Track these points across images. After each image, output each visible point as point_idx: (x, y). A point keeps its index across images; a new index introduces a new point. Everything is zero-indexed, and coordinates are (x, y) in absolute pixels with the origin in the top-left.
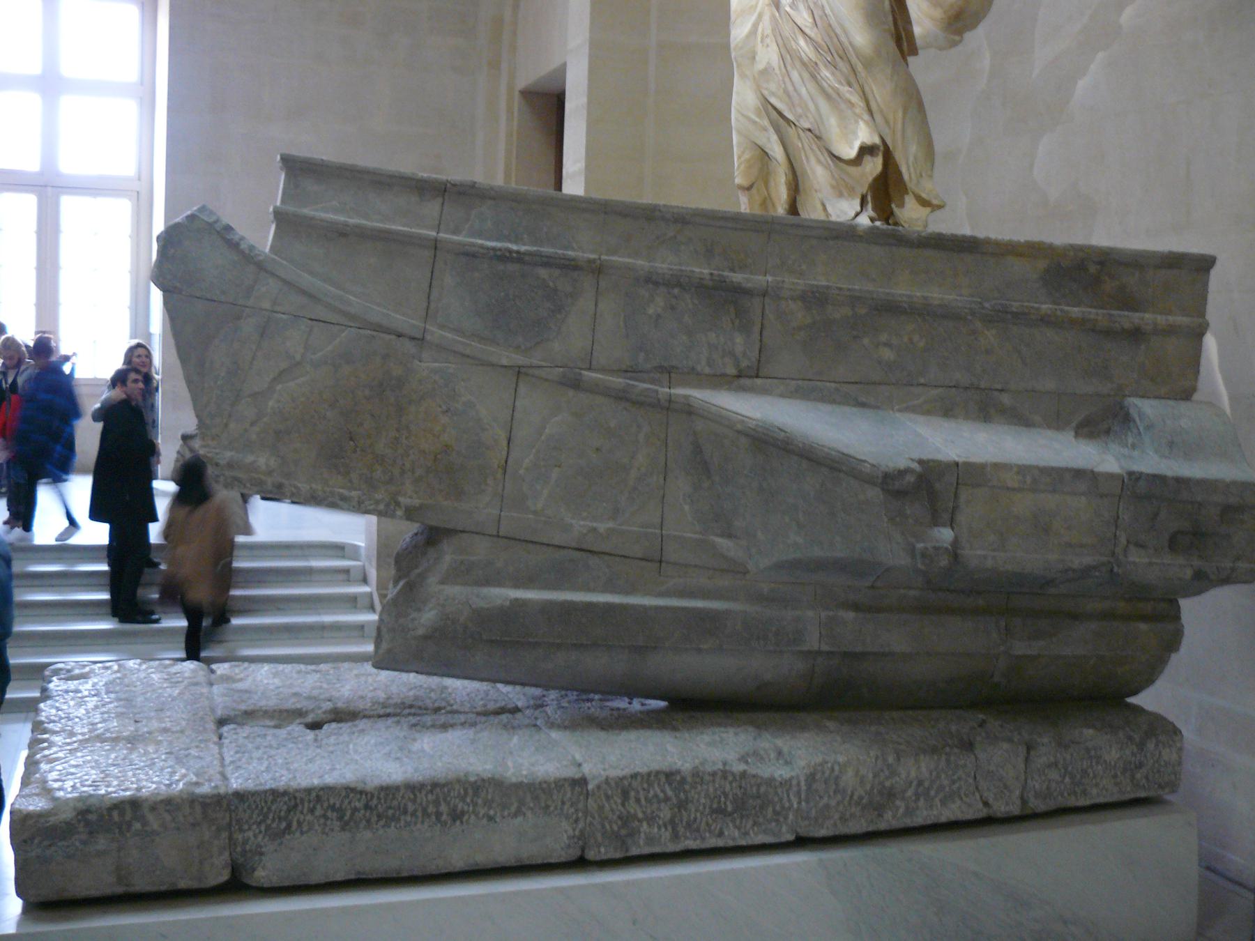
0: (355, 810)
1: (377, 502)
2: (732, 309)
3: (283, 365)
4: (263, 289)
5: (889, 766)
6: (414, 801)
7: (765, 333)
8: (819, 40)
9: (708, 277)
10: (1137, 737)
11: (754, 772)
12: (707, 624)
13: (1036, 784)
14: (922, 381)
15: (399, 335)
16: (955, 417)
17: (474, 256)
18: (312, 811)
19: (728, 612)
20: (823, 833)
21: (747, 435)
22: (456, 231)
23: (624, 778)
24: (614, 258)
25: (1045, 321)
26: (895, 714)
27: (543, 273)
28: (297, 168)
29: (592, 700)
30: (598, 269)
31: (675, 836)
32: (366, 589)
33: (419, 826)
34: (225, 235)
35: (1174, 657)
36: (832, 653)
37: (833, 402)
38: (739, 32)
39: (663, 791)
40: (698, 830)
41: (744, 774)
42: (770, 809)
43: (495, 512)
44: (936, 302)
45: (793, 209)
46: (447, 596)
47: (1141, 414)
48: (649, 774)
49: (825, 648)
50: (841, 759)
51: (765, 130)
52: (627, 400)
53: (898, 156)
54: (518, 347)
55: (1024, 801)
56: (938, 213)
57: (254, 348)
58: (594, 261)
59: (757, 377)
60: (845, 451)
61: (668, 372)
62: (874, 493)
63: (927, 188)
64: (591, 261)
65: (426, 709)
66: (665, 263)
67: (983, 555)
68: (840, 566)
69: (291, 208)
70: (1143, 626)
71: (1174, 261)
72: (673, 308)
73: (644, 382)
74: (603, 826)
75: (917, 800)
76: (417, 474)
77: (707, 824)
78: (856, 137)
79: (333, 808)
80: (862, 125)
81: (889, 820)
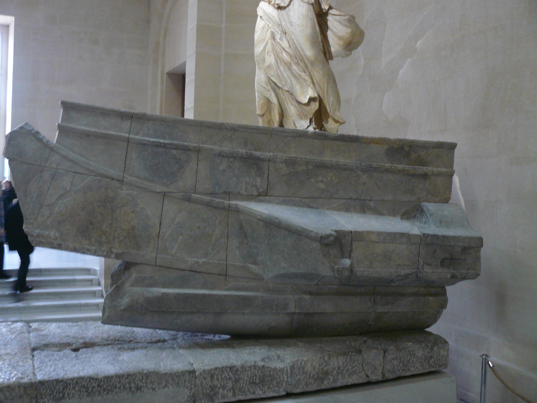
0: (94, 387)
1: (103, 251)
2: (256, 167)
5: (325, 361)
6: (120, 382)
7: (270, 177)
8: (291, 53)
10: (430, 346)
11: (268, 366)
12: (247, 302)
13: (388, 367)
14: (336, 197)
15: (112, 179)
16: (350, 212)
17: (144, 145)
18: (74, 388)
19: (255, 297)
20: (298, 391)
21: (262, 221)
22: (137, 134)
23: (212, 369)
24: (205, 146)
25: (388, 171)
26: (328, 339)
27: (174, 152)
28: (68, 107)
29: (198, 336)
30: (198, 151)
31: (234, 394)
32: (100, 288)
33: (122, 393)
34: (36, 135)
35: (444, 311)
36: (301, 313)
37: (299, 206)
38: (258, 50)
39: (228, 375)
40: (244, 391)
41: (263, 367)
42: (275, 381)
43: (154, 255)
44: (342, 163)
45: (281, 125)
46: (134, 292)
48: (222, 368)
49: (297, 311)
50: (305, 359)
51: (269, 91)
52: (211, 206)
53: (325, 102)
54: (164, 184)
55: (383, 374)
56: (342, 126)
58: (196, 147)
59: (266, 195)
60: (304, 227)
61: (228, 194)
62: (316, 245)
63: (338, 115)
65: (125, 341)
66: (227, 148)
67: (362, 270)
68: (303, 276)
69: (65, 124)
70: (431, 298)
71: (440, 145)
72: (230, 167)
73: (218, 198)
74: (203, 391)
75: (338, 376)
76: (120, 239)
77: (248, 389)
78: (308, 94)
79: (83, 386)
80: (310, 89)
81: (326, 385)
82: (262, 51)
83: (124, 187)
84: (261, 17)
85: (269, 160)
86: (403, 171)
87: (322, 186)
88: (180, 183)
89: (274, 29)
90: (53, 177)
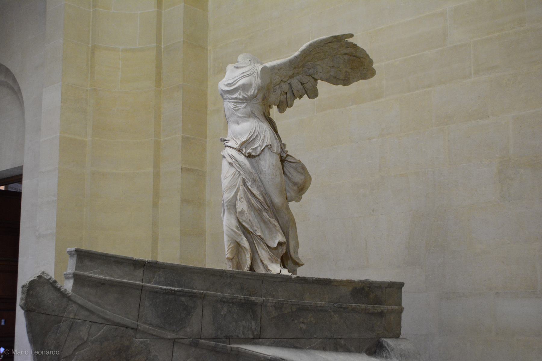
3: (79, 343)
4: (71, 309)
9: (243, 299)
14: (315, 336)
22: (149, 282)
25: (354, 310)
27: (183, 299)
30: (203, 297)
34: (53, 284)
47: (388, 345)
54: (174, 331)
57: (66, 335)
58: (202, 294)
59: (260, 338)
61: (229, 338)
64: (201, 294)
66: (227, 294)
80: (279, 235)
82: (233, 197)
83: (138, 336)
84: (230, 163)
85: (262, 305)
86: (366, 309)
87: (303, 326)
88: (188, 330)
89: (246, 177)
90: (71, 328)
